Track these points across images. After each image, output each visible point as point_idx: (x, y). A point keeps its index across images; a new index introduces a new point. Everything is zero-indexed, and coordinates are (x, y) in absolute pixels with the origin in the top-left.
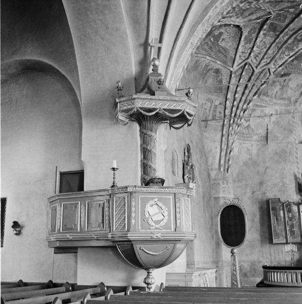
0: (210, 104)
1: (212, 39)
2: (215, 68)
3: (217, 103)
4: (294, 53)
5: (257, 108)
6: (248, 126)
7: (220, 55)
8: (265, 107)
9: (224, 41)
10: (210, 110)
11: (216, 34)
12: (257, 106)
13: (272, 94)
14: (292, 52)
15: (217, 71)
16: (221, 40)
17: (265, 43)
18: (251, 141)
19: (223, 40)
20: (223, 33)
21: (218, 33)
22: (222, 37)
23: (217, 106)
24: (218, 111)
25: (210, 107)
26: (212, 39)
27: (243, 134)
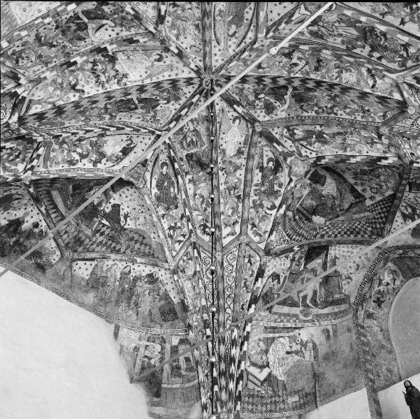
0: (158, 348)
1: (104, 221)
2: (144, 274)
3: (175, 341)
4: (280, 199)
5: (277, 335)
6: (270, 379)
7: (137, 246)
8: (295, 328)
9: (128, 219)
10: (162, 359)
11: (107, 211)
12: (274, 329)
13: (305, 297)
14: (276, 198)
15: (152, 279)
16: (122, 219)
17: (203, 197)
18: (284, 410)
19: (126, 216)
20: (119, 206)
21: (110, 209)
22: (122, 212)
23: (176, 347)
24: (182, 359)
25: (162, 353)
26: (104, 221)
27: (262, 397)
